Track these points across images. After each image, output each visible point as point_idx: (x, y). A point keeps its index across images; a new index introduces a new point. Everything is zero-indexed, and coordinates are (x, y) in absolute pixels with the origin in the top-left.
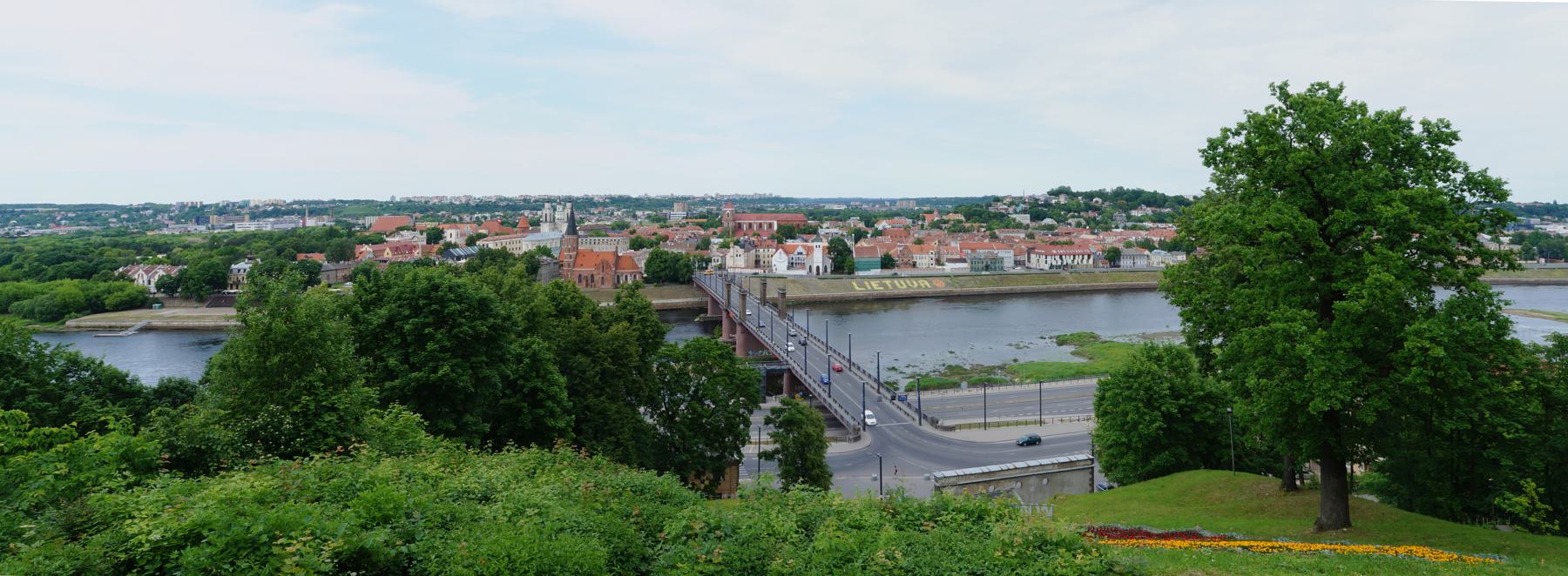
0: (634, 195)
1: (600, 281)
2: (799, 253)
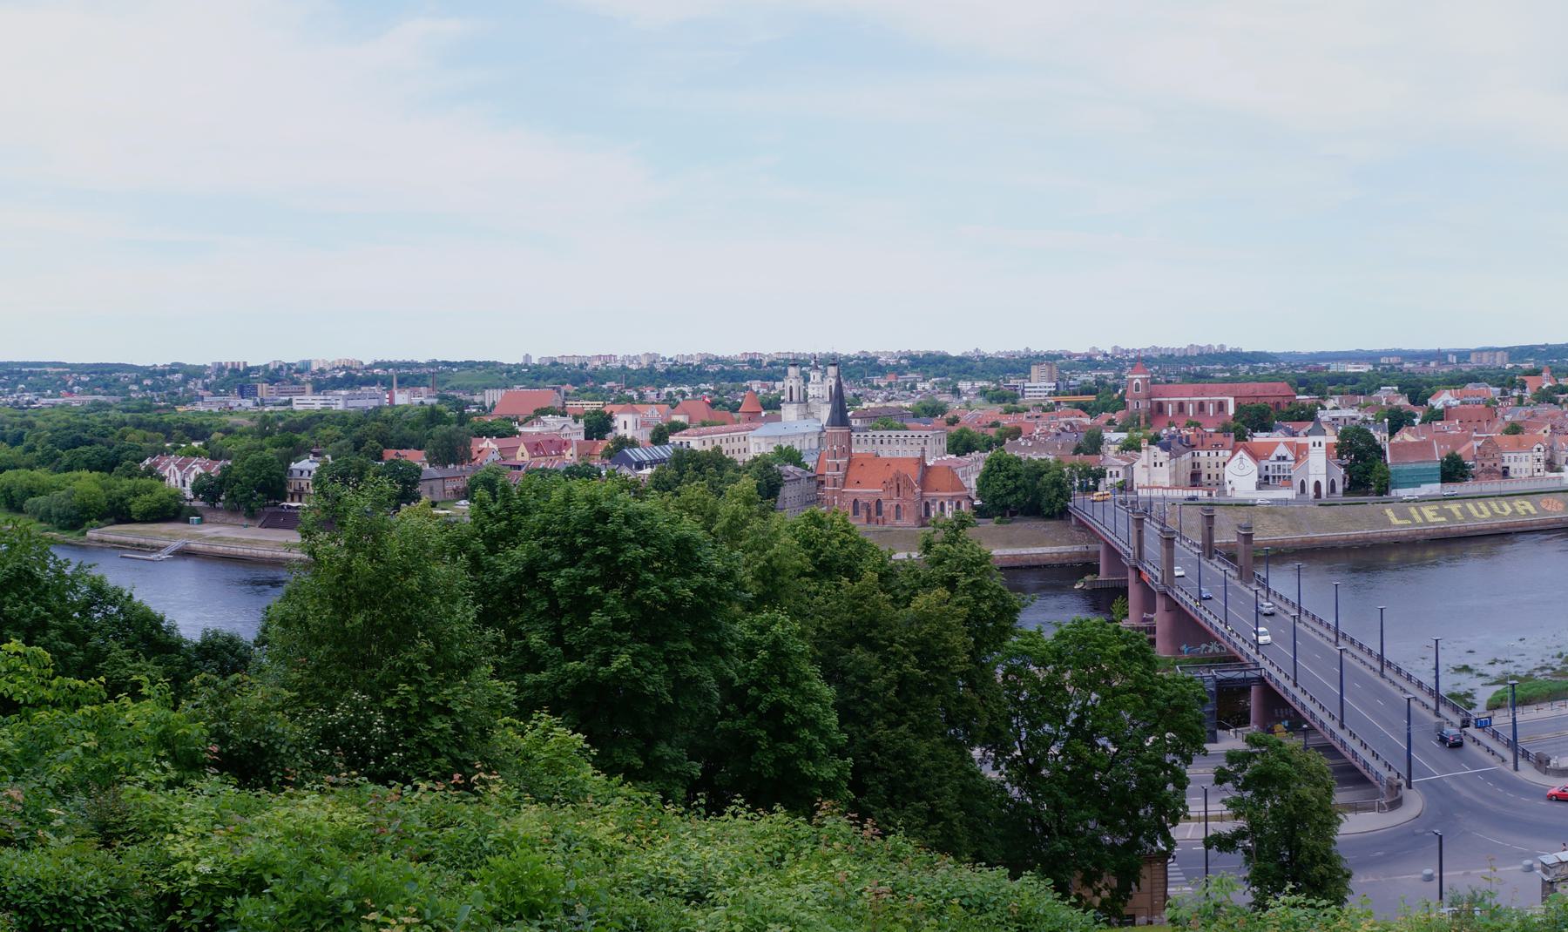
0: (955, 352)
2: (1279, 458)
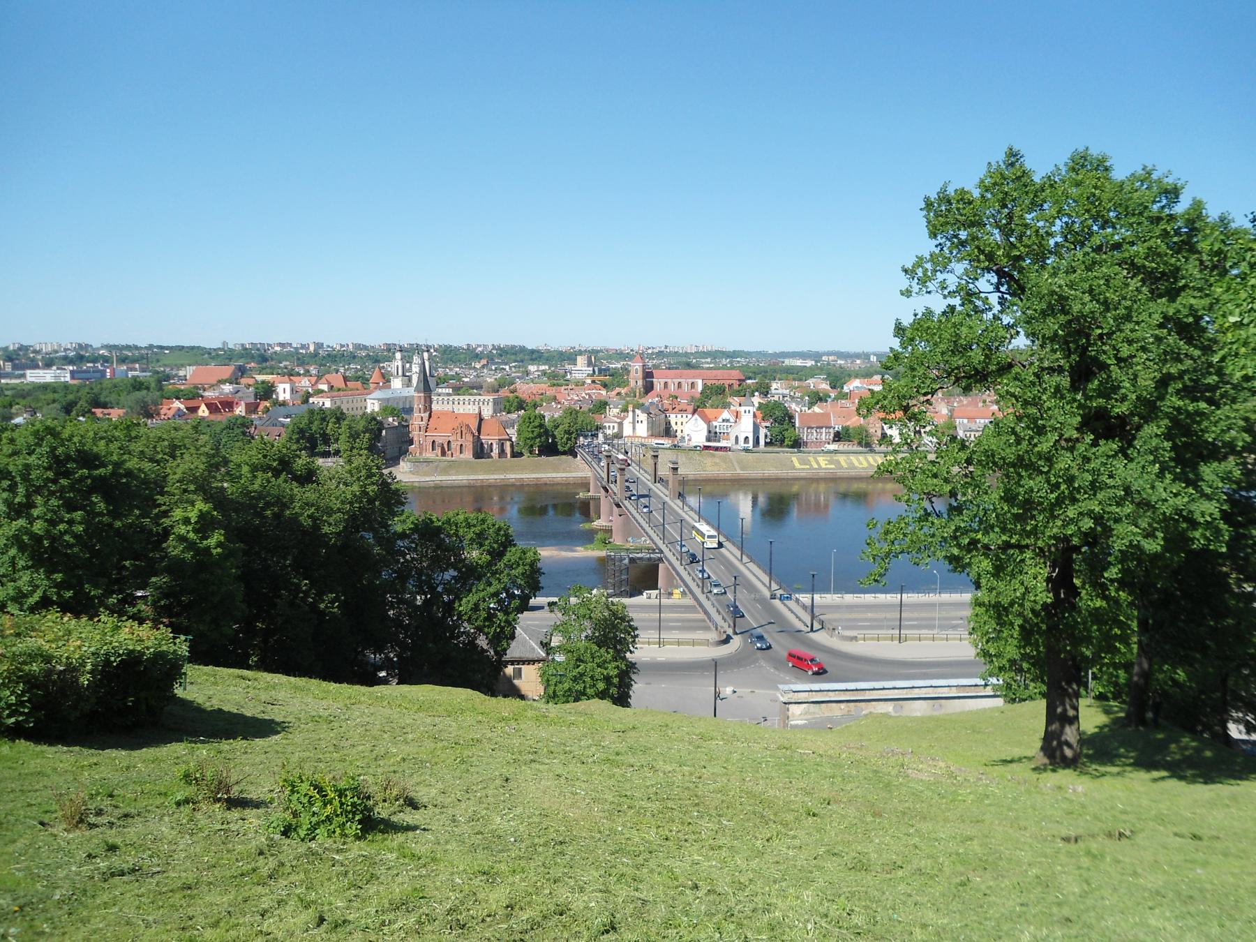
0: (530, 346)
1: (458, 448)
2: (724, 420)
